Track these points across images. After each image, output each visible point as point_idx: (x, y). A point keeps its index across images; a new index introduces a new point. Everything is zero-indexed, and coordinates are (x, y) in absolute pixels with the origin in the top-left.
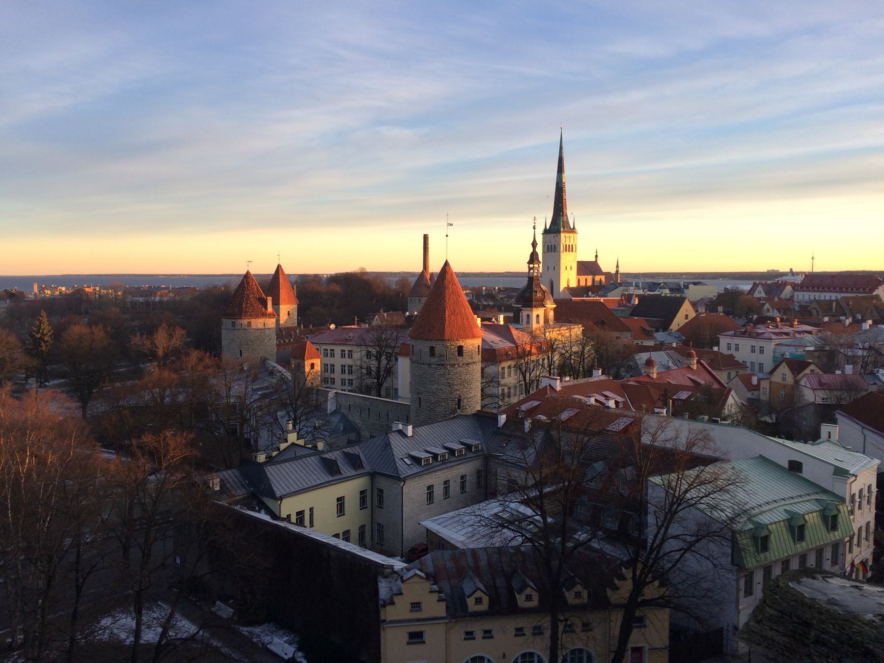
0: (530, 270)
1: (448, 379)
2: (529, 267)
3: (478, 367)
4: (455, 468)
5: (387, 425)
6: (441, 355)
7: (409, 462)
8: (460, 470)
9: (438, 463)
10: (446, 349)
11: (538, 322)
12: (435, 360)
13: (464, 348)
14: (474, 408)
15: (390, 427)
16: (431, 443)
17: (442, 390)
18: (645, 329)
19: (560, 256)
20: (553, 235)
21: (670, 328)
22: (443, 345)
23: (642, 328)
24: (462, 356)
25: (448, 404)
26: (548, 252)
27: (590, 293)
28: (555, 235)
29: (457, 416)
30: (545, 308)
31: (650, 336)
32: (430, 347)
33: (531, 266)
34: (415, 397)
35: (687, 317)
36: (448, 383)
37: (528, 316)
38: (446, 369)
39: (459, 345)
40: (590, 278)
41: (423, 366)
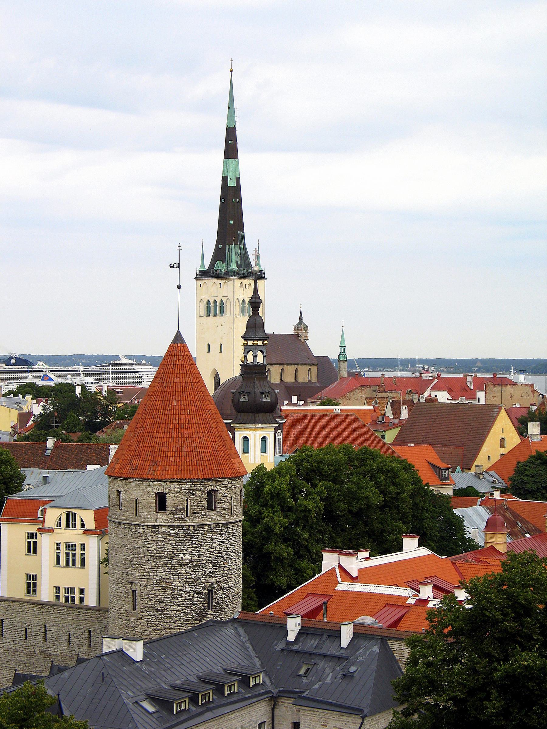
0: (246, 353)
1: (190, 553)
2: (245, 345)
3: (239, 530)
4: (226, 718)
5: (42, 652)
6: (177, 509)
7: (151, 709)
8: (233, 722)
9: (200, 710)
10: (185, 497)
11: (263, 450)
12: (165, 518)
13: (219, 495)
14: (234, 607)
15: (50, 655)
16: (177, 673)
17: (179, 574)
18: (433, 466)
19: (233, 324)
20: (218, 281)
21: (476, 463)
22: (181, 489)
23: (429, 462)
24: (215, 510)
25: (190, 600)
26: (209, 315)
27: (295, 399)
28: (222, 281)
29: (207, 622)
30: (277, 425)
31: (445, 479)
32: (157, 494)
33: (250, 343)
34: (122, 589)
35: (503, 440)
36: (191, 560)
37: (246, 439)
38: (186, 536)
39: (210, 488)
40: (290, 369)
41: (141, 530)
